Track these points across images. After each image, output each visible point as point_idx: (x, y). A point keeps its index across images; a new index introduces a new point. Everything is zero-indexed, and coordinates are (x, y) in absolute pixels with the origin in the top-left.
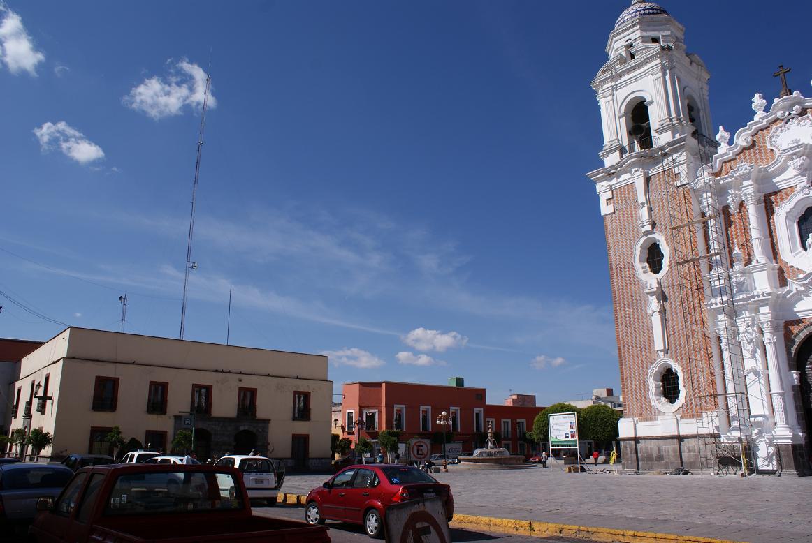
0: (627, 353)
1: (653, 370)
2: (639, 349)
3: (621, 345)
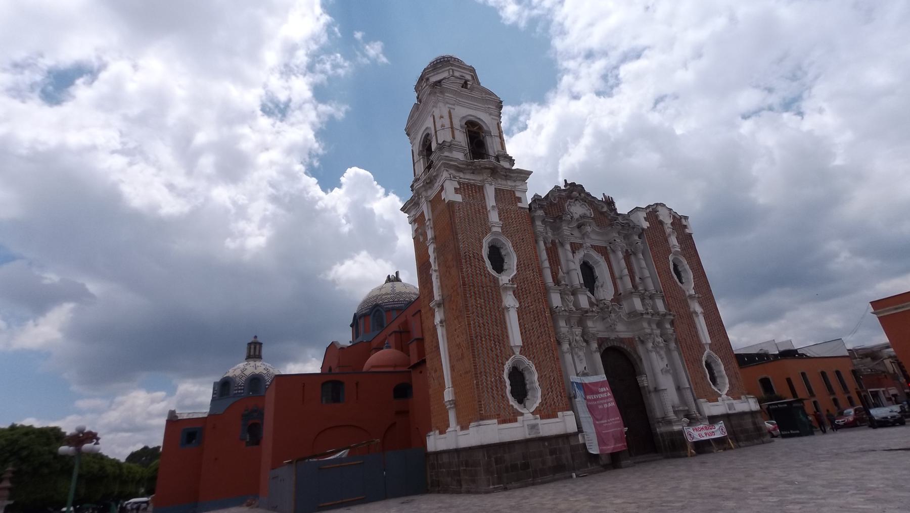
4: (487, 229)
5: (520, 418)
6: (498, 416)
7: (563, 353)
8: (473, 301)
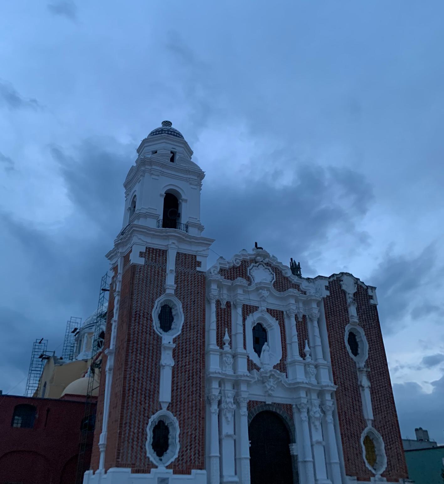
0: (131, 397)
1: (154, 418)
2: (143, 396)
3: (127, 388)
4: (162, 290)
5: (153, 470)
6: (132, 466)
7: (211, 413)
8: (134, 356)
